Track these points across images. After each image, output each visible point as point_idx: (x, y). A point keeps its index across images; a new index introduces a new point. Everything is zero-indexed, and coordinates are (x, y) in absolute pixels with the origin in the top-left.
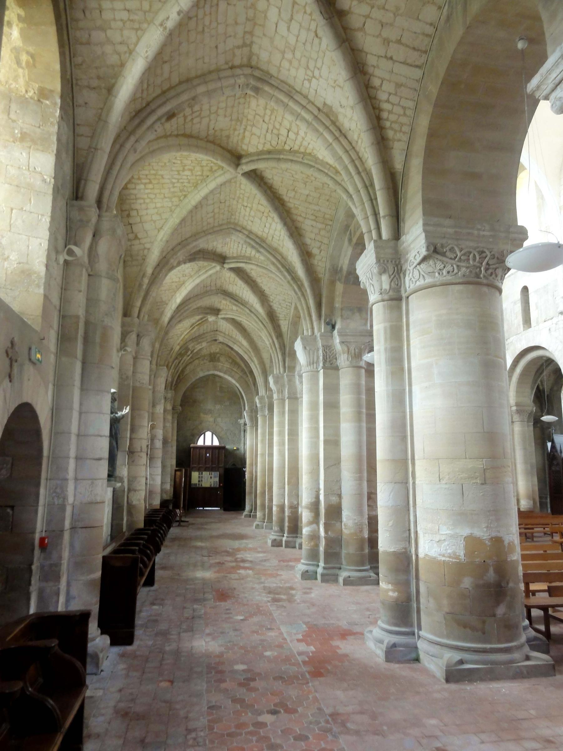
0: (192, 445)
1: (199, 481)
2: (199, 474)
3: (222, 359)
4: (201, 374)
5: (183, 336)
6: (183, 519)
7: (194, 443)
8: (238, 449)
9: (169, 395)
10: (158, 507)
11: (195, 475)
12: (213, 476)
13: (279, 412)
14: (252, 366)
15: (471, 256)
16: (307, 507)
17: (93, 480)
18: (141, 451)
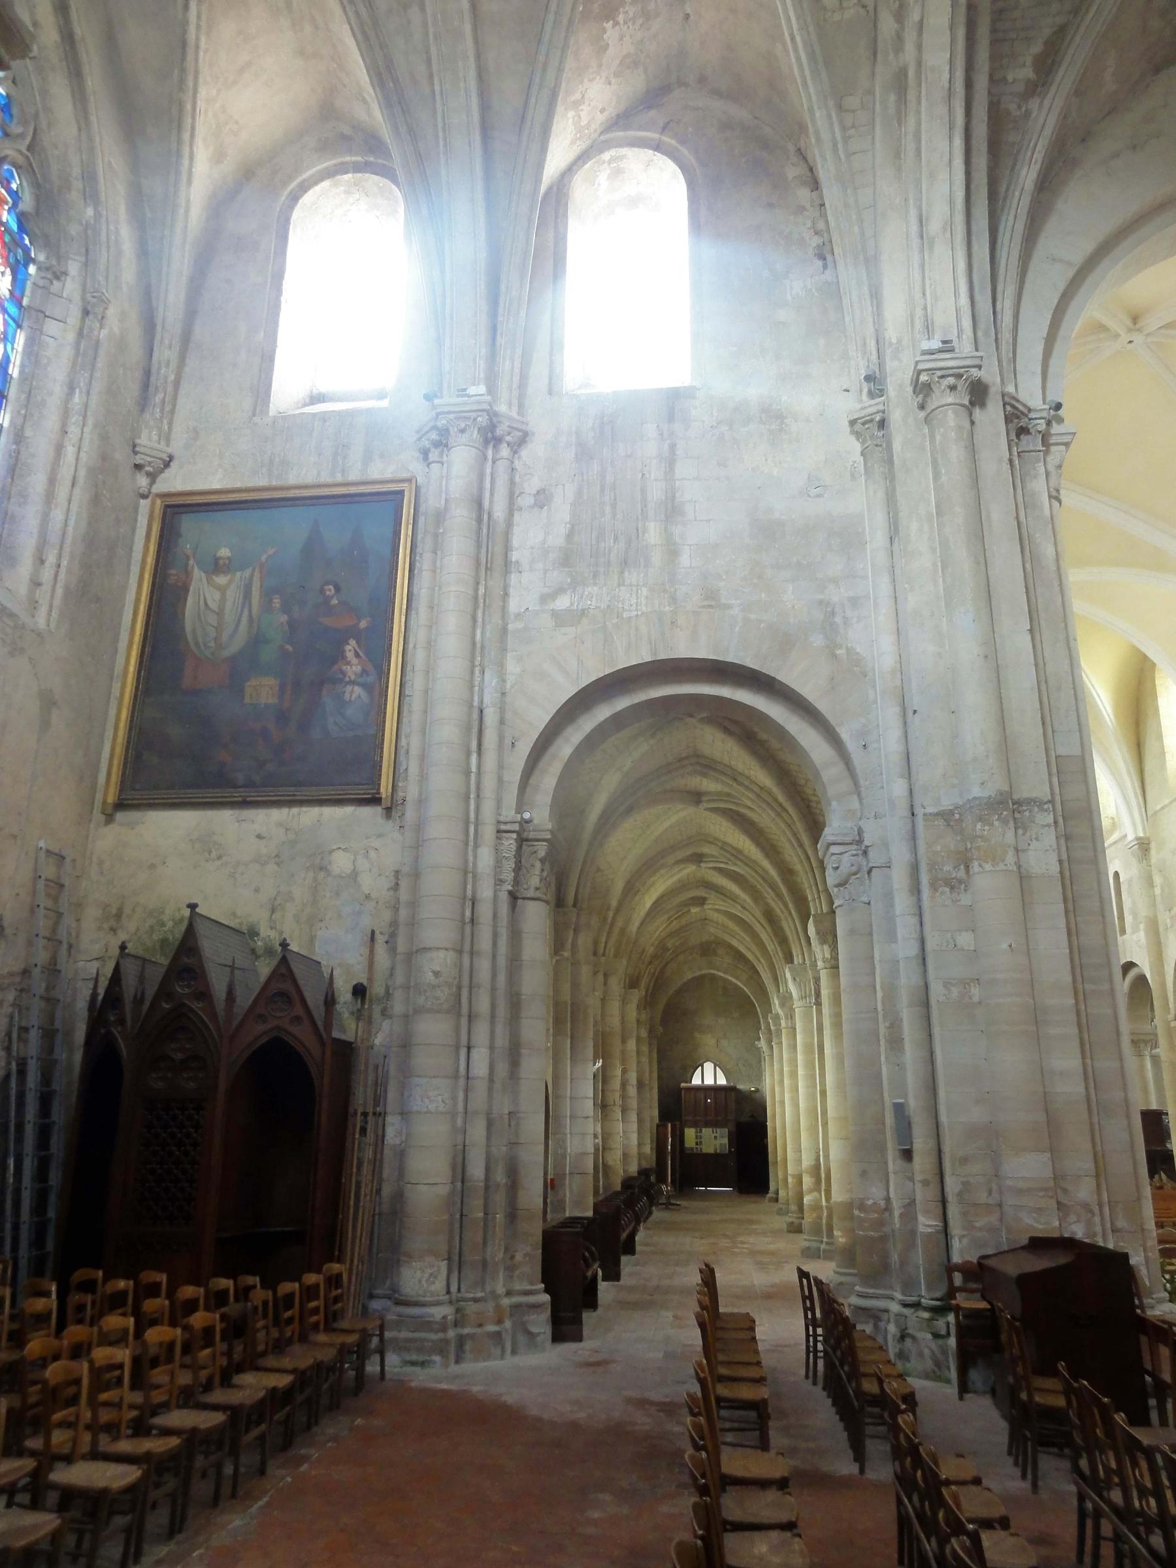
0: (683, 1085)
1: (697, 1144)
2: (696, 1132)
3: (720, 951)
4: (689, 975)
5: (657, 933)
6: (673, 1201)
7: (686, 1082)
8: (757, 1091)
9: (643, 1017)
10: (636, 1174)
11: (690, 1133)
12: (717, 1135)
13: (789, 1045)
14: (760, 968)
16: (807, 1173)
17: (584, 1134)
18: (614, 1105)
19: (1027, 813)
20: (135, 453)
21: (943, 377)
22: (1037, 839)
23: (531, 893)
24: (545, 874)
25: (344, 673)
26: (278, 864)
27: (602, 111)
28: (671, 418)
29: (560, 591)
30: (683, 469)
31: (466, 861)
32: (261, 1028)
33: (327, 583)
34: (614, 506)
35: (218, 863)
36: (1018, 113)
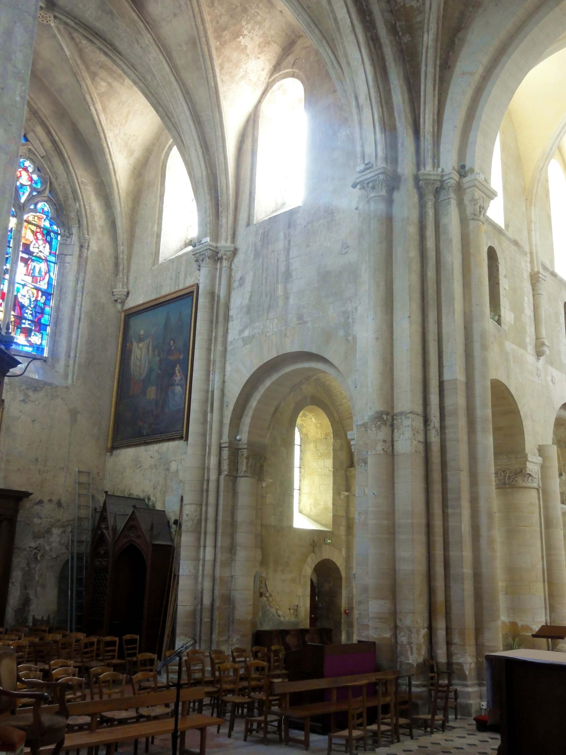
15: (499, 473)
19: (399, 420)
20: (114, 295)
21: (368, 183)
22: (403, 434)
23: (242, 474)
24: (249, 464)
25: (175, 380)
26: (156, 468)
27: (263, 70)
28: (289, 227)
29: (246, 327)
30: (294, 252)
31: (204, 463)
32: (125, 540)
33: (171, 340)
34: (266, 279)
35: (139, 469)
36: (419, 5)
